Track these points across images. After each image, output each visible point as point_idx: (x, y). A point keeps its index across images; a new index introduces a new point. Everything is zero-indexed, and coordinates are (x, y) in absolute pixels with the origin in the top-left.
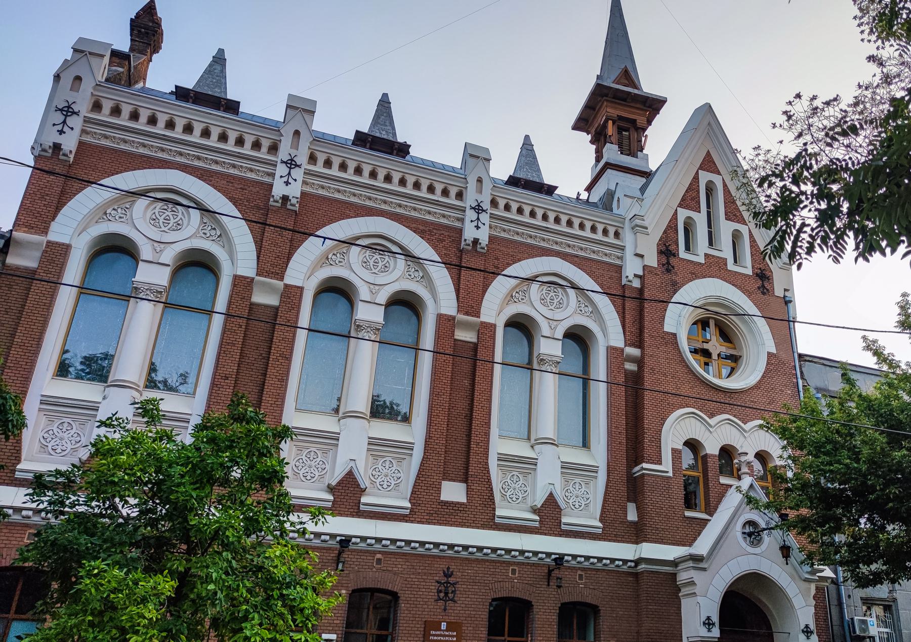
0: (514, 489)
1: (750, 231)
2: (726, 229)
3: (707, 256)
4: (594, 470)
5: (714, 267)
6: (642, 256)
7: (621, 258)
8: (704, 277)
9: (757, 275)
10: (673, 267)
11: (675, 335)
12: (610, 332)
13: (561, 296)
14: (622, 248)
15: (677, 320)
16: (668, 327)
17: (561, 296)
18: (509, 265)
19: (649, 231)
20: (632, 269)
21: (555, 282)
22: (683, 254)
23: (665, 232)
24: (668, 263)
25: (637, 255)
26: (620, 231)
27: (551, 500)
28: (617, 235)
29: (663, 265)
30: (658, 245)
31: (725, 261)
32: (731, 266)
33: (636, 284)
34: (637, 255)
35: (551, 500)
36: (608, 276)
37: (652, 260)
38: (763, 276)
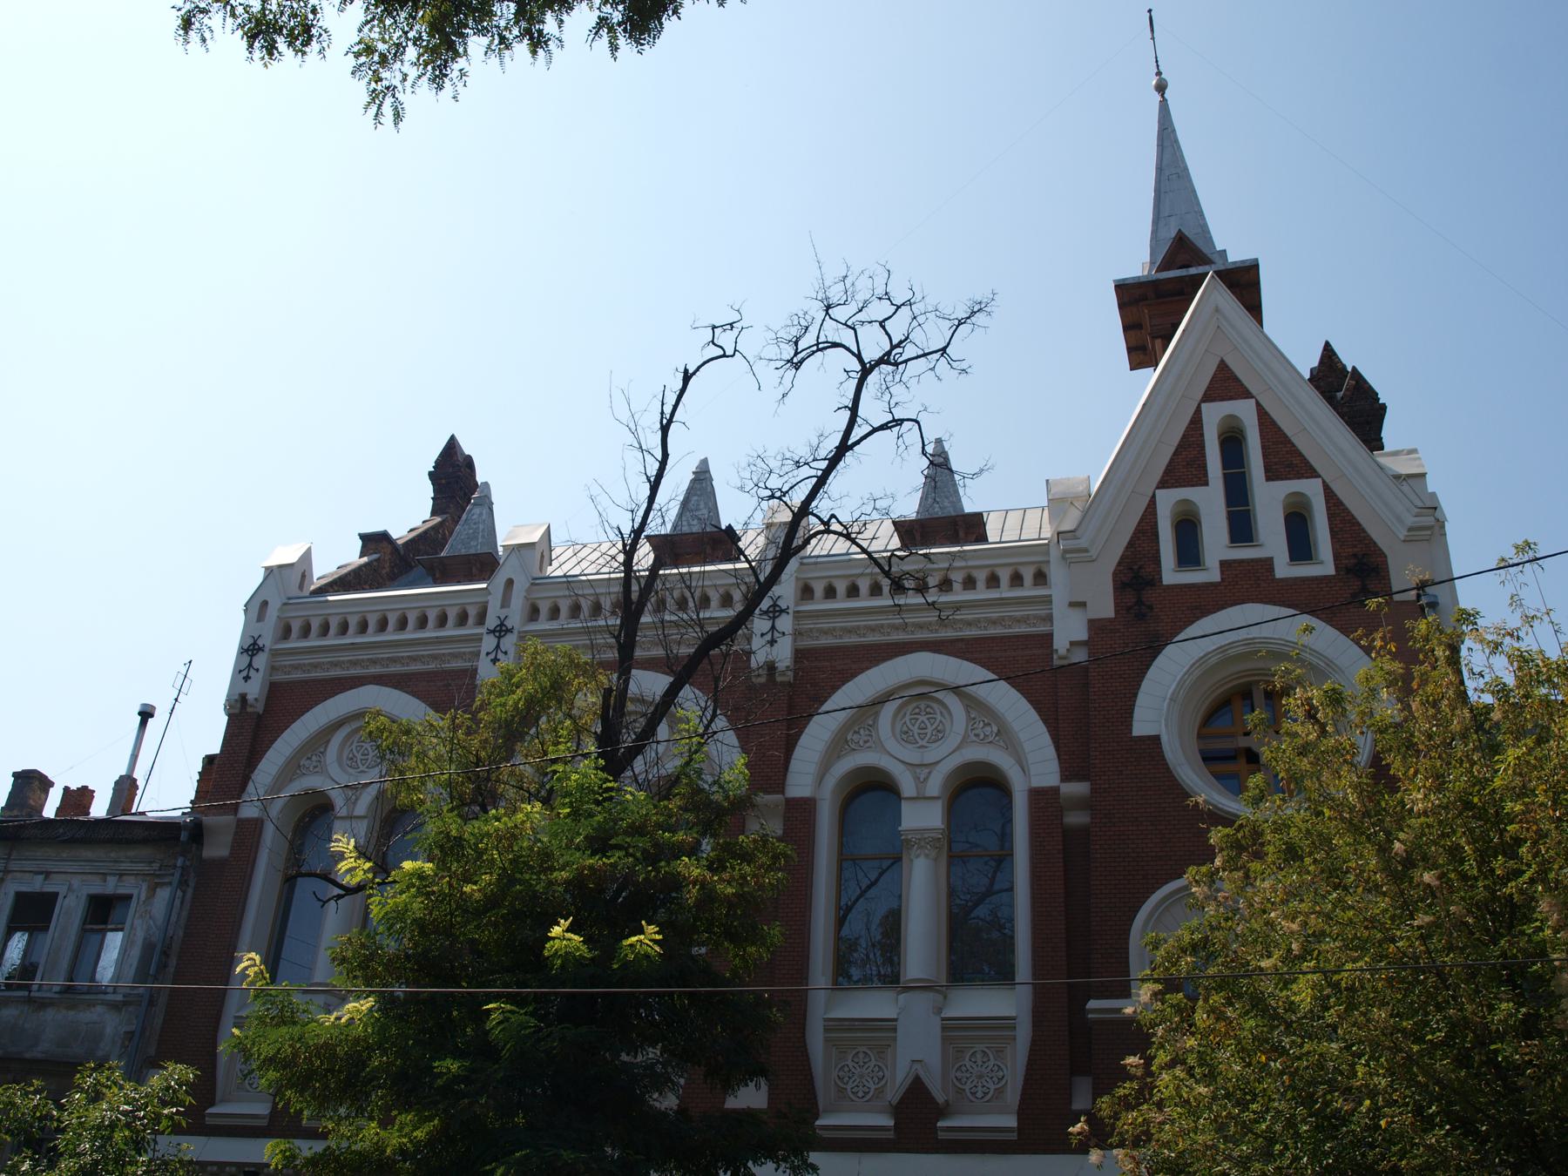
0: (861, 1076)
1: (1326, 488)
2: (1269, 500)
3: (1225, 565)
4: (1004, 1025)
5: (1248, 582)
6: (1083, 605)
7: (1049, 619)
8: (1223, 608)
9: (1348, 570)
10: (1151, 608)
11: (1156, 740)
12: (1032, 758)
13: (939, 717)
14: (1047, 600)
15: (1160, 703)
16: (1140, 728)
17: (939, 717)
18: (835, 689)
19: (1093, 553)
20: (1068, 631)
21: (922, 694)
22: (1171, 574)
23: (1130, 544)
24: (1139, 602)
25: (1072, 605)
26: (1045, 569)
27: (917, 1089)
28: (1041, 578)
29: (1129, 609)
30: (1115, 574)
31: (1268, 564)
32: (1284, 569)
33: (1080, 656)
34: (1072, 605)
35: (917, 1089)
36: (1019, 658)
37: (1104, 607)
38: (1363, 565)
